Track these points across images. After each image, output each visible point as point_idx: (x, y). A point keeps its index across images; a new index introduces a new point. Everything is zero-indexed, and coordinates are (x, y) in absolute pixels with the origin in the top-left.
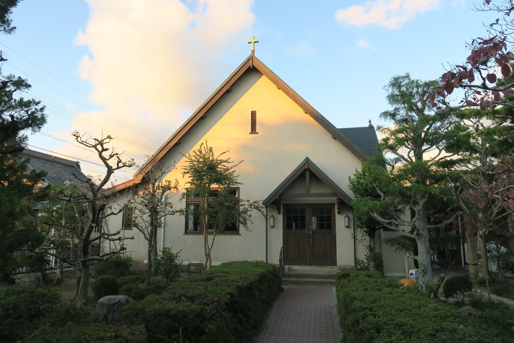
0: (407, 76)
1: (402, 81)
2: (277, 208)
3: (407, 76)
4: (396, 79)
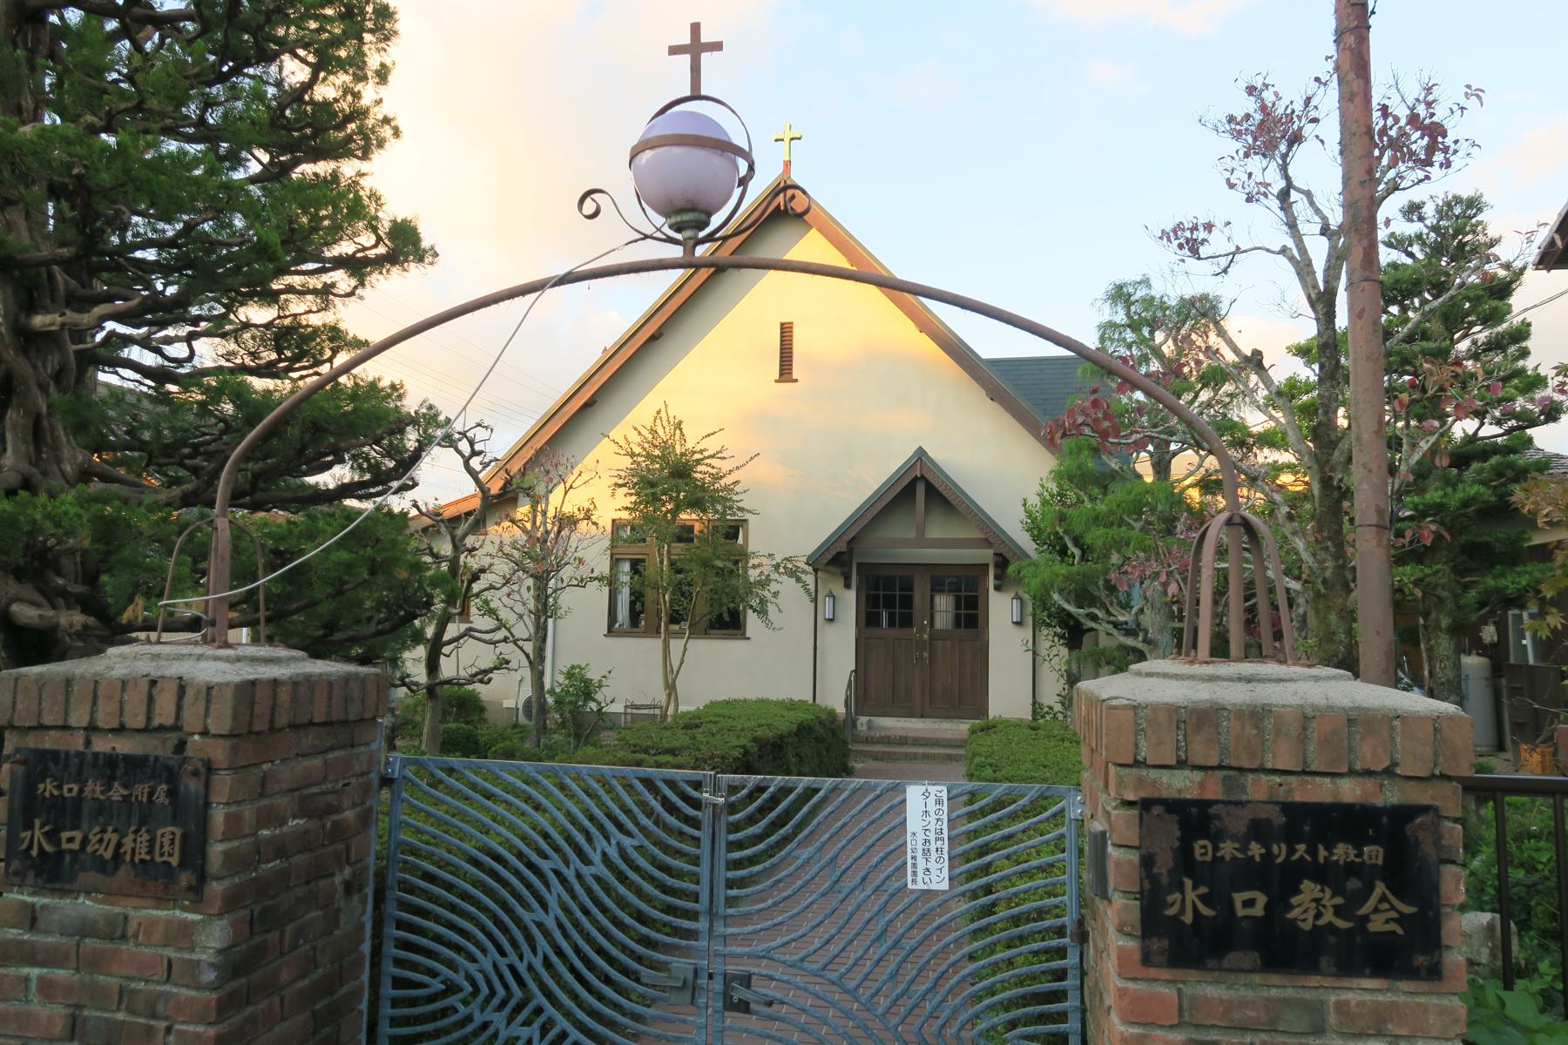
0: (1146, 282)
1: (1131, 290)
2: (779, 823)
3: (1146, 282)
4: (1120, 288)
